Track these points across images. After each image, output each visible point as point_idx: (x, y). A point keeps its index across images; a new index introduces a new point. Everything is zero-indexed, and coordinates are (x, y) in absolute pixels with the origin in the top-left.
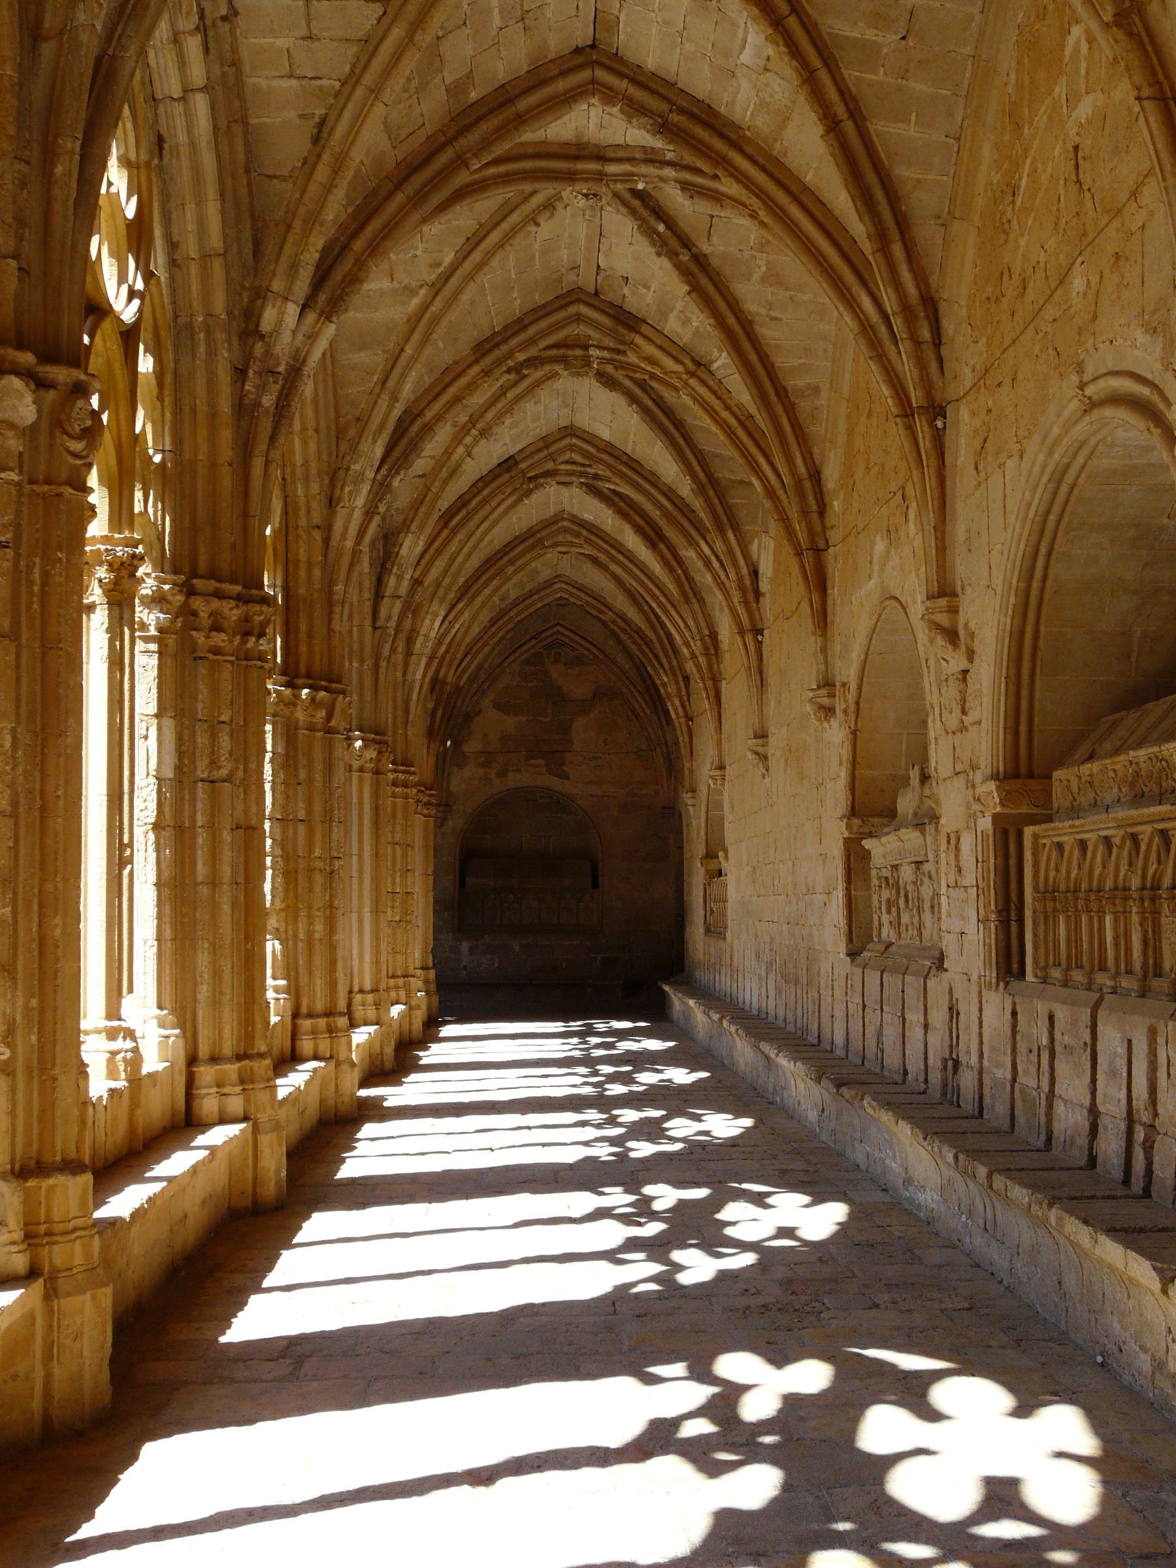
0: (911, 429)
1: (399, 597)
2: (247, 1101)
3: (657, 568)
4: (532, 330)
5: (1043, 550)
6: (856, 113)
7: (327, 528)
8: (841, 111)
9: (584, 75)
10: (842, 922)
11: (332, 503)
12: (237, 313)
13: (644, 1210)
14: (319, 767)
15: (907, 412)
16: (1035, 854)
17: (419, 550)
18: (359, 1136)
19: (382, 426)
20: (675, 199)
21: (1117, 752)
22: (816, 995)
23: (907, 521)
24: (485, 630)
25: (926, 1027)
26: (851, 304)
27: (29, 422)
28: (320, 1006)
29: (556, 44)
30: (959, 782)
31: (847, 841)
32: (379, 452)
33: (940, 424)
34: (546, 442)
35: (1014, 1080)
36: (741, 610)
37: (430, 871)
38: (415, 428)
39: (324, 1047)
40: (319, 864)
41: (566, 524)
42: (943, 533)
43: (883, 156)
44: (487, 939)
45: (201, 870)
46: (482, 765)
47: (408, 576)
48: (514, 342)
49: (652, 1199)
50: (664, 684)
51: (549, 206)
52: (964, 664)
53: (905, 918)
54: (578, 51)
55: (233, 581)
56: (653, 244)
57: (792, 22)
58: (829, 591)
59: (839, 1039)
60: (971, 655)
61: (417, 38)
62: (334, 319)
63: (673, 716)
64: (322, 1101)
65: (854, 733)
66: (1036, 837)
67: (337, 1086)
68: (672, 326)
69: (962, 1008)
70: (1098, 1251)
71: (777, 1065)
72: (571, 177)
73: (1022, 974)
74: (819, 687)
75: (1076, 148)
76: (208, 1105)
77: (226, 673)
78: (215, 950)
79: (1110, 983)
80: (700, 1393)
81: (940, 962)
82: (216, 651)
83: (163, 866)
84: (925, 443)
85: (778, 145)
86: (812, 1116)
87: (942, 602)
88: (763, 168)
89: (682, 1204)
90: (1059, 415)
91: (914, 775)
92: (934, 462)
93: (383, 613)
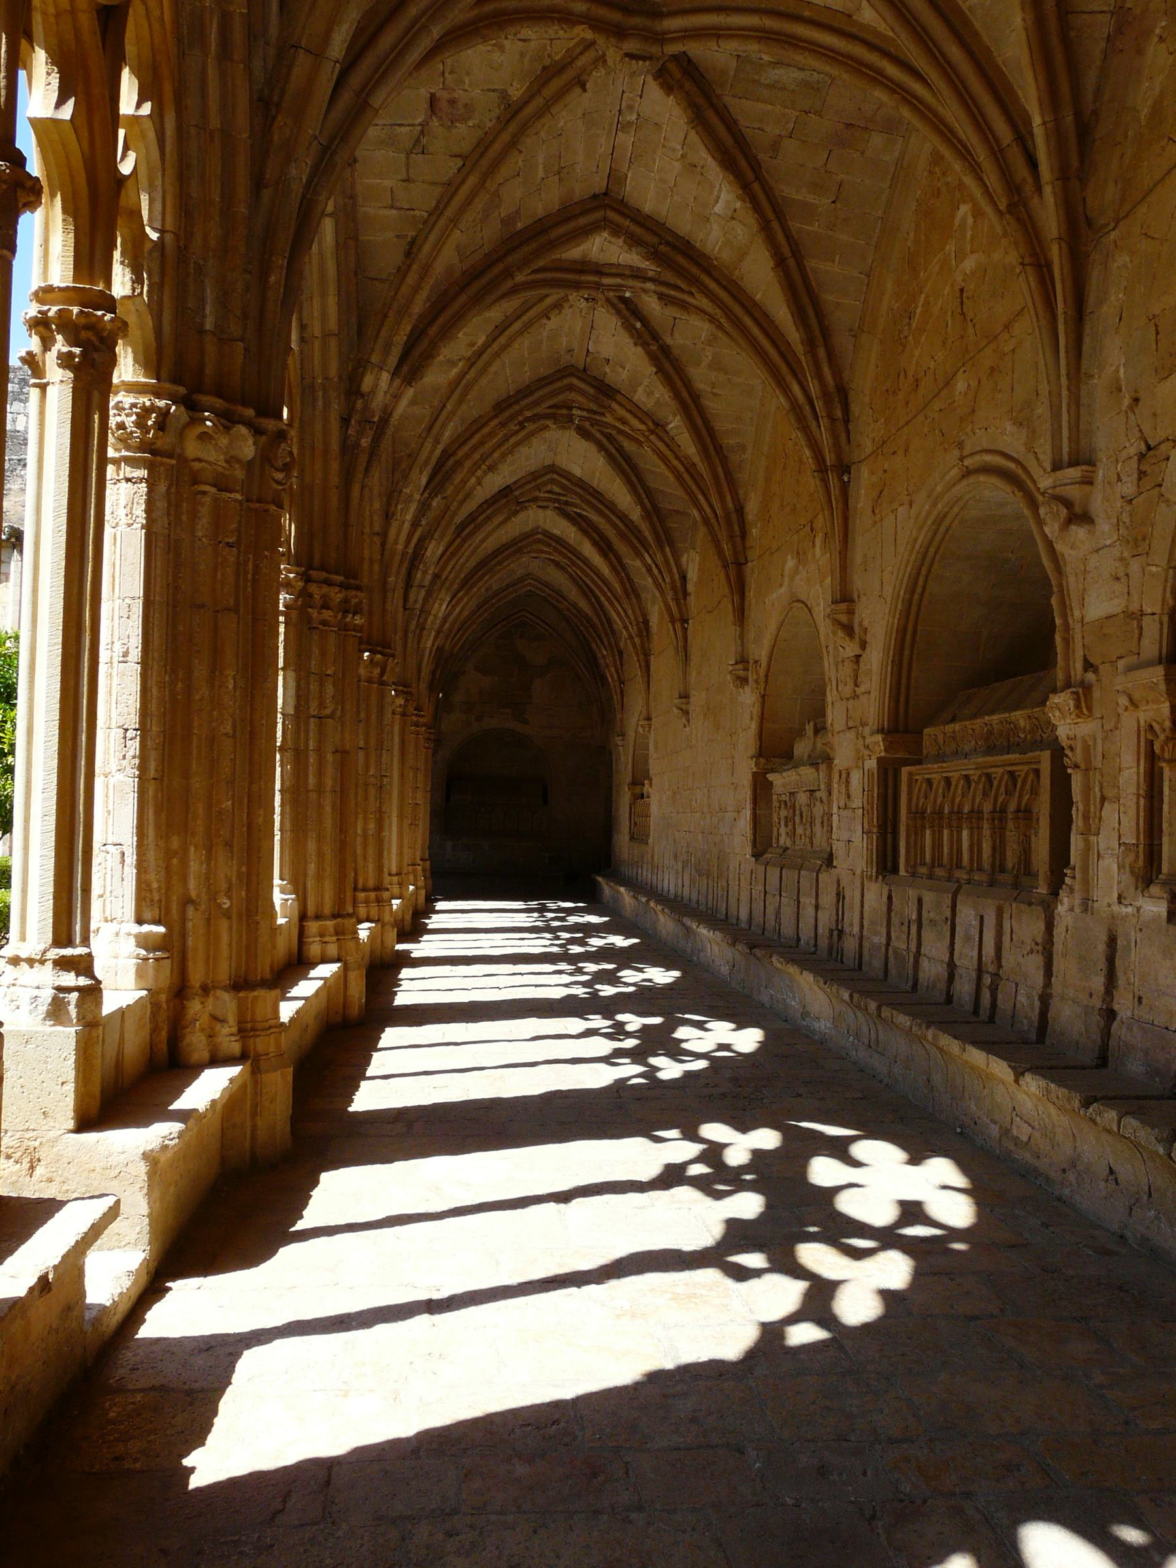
0: (825, 481)
1: (424, 587)
2: (340, 948)
3: (606, 571)
4: (538, 394)
5: (924, 572)
6: (797, 254)
7: (384, 535)
9: (600, 214)
10: (749, 834)
11: (388, 516)
12: (344, 377)
13: (619, 1031)
14: (374, 710)
15: (822, 468)
16: (910, 786)
17: (440, 552)
18: (400, 976)
19: (426, 462)
20: (651, 304)
21: (974, 716)
22: (725, 884)
23: (814, 546)
24: (473, 612)
25: (817, 907)
26: (786, 391)
27: (249, 458)
28: (371, 883)
29: (580, 191)
30: (851, 735)
31: (754, 774)
32: (424, 481)
33: (846, 479)
34: (534, 476)
35: (888, 944)
36: (672, 604)
37: (429, 788)
38: (450, 463)
39: (374, 912)
40: (372, 780)
41: (540, 536)
42: (846, 555)
43: (813, 284)
45: (312, 780)
47: (431, 572)
48: (524, 403)
49: (624, 1023)
50: (604, 657)
51: (558, 306)
52: (858, 651)
53: (799, 831)
54: (595, 196)
55: (337, 573)
56: (632, 336)
57: (756, 186)
58: (747, 594)
59: (744, 915)
60: (863, 645)
61: (488, 184)
62: (413, 384)
63: (610, 680)
64: (372, 952)
65: (763, 696)
66: (910, 774)
67: (382, 941)
68: (640, 396)
69: (847, 893)
70: (965, 1056)
71: (695, 933)
72: (577, 286)
73: (895, 870)
74: (737, 663)
75: (962, 290)
76: (314, 949)
77: (332, 640)
78: (320, 839)
79: (965, 876)
80: (693, 1149)
81: (829, 861)
82: (325, 623)
83: (285, 777)
84: (835, 492)
85: (737, 273)
86: (725, 970)
87: (844, 606)
88: (725, 288)
89: (645, 1028)
90: (942, 478)
91: (809, 728)
92: (840, 505)
93: (412, 597)
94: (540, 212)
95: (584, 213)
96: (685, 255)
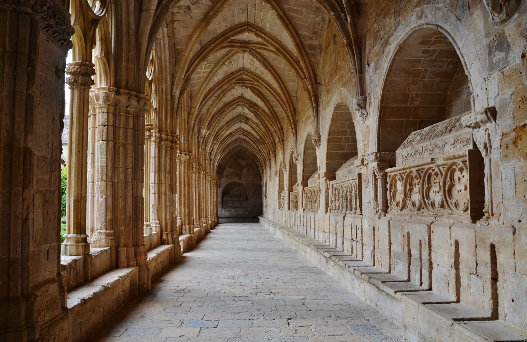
3: (255, 147)
7: (205, 149)
8: (270, 107)
11: (206, 146)
32: (212, 139)
34: (237, 130)
44: (227, 209)
46: (227, 178)
51: (236, 108)
57: (264, 99)
93: (211, 157)
94: (230, 100)
95: (237, 99)
96: (255, 106)
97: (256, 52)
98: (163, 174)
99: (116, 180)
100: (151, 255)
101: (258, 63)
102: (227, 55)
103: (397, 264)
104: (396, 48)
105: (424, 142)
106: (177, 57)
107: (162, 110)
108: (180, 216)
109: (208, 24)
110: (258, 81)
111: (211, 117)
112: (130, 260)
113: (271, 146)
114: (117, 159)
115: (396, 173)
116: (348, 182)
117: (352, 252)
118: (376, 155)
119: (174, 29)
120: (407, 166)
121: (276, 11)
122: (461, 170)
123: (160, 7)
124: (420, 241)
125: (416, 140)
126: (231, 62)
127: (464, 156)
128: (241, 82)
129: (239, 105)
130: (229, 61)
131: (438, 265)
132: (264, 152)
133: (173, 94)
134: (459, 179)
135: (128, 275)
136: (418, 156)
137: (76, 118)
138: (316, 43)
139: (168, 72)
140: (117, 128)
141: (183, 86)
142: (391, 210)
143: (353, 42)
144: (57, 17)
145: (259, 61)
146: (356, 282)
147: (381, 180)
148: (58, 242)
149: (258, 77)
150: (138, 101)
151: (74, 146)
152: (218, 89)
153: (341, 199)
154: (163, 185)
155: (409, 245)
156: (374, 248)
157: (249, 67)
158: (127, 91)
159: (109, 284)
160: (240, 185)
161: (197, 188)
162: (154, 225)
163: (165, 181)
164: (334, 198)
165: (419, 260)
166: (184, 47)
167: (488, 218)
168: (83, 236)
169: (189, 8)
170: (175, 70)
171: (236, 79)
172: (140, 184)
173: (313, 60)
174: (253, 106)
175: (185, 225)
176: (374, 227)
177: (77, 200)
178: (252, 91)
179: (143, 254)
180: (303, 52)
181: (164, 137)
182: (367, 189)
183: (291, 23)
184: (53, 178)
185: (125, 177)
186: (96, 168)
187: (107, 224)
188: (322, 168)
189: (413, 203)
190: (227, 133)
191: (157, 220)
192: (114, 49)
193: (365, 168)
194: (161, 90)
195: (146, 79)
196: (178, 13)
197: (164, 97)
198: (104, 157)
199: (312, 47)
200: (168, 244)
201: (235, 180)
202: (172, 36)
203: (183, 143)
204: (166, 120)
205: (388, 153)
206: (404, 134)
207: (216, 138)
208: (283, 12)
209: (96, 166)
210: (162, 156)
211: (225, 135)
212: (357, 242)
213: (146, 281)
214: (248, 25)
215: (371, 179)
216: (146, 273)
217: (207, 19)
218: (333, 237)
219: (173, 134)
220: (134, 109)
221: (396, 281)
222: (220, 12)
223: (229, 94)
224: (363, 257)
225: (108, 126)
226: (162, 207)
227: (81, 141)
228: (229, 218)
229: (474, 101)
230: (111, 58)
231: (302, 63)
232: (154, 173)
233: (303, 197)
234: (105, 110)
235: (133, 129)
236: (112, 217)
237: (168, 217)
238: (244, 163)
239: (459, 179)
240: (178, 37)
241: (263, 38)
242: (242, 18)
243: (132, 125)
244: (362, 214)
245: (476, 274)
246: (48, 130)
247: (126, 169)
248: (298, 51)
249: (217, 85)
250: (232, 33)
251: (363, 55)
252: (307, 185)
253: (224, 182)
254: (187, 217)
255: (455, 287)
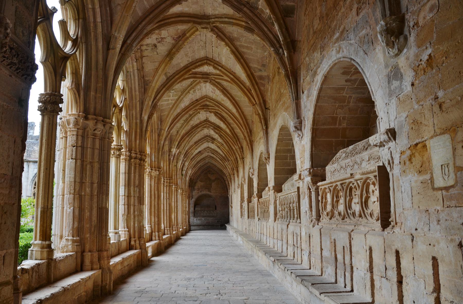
3: (222, 163)
7: (176, 166)
11: (177, 162)
24: (198, 170)
32: (183, 156)
34: (205, 149)
44: (199, 218)
51: (203, 129)
57: (226, 122)
84: (242, 162)
93: (183, 172)
94: (197, 123)
97: (216, 82)
98: (132, 187)
99: (83, 194)
100: (117, 259)
101: (218, 91)
102: (192, 85)
103: (327, 268)
104: (322, 78)
105: (347, 159)
106: (146, 87)
107: (132, 132)
108: (150, 225)
109: (171, 59)
110: (219, 107)
111: (180, 138)
112: (94, 264)
113: (234, 163)
114: (84, 175)
115: (325, 186)
116: (291, 194)
117: (294, 257)
118: (310, 171)
119: (143, 63)
120: (333, 180)
121: (229, 47)
122: (374, 184)
123: (125, 46)
124: (344, 247)
125: (342, 157)
126: (195, 90)
127: (374, 171)
128: (205, 107)
129: (205, 127)
130: (193, 90)
131: (357, 268)
132: (229, 168)
133: (142, 119)
134: (373, 192)
135: (90, 277)
136: (342, 171)
137: (45, 140)
138: (264, 74)
139: (138, 99)
140: (85, 149)
141: (150, 112)
142: (322, 219)
143: (290, 73)
144: (20, 56)
145: (219, 90)
146: (295, 284)
147: (314, 192)
148: (15, 248)
149: (219, 104)
150: (104, 125)
151: (43, 164)
152: (185, 114)
153: (286, 209)
154: (132, 197)
155: (335, 251)
156: (310, 253)
157: (211, 95)
158: (95, 117)
159: (68, 285)
160: (210, 196)
161: (168, 200)
162: (123, 233)
163: (134, 194)
164: (281, 208)
165: (343, 265)
166: (151, 79)
167: (393, 226)
168: (47, 243)
169: (155, 46)
170: (144, 98)
171: (200, 105)
172: (104, 197)
173: (262, 88)
174: (216, 128)
175: (155, 232)
176: (309, 234)
177: (44, 211)
178: (216, 115)
179: (106, 259)
180: (254, 81)
181: (133, 155)
182: (304, 201)
183: (242, 57)
184: (13, 193)
185: (92, 191)
186: (66, 183)
187: (74, 232)
188: (271, 183)
189: (339, 213)
190: (197, 151)
191: (126, 228)
192: (84, 81)
193: (302, 182)
194: (131, 115)
195: (116, 106)
196: (147, 50)
197: (134, 121)
198: (73, 173)
199: (261, 78)
200: (136, 249)
201: (204, 192)
202: (141, 69)
203: (153, 160)
204: (136, 141)
205: (320, 168)
206: (334, 152)
207: (186, 156)
208: (235, 48)
209: (66, 181)
210: (131, 172)
211: (195, 154)
212: (298, 247)
213: (108, 282)
214: (207, 60)
215: (307, 192)
216: (108, 275)
217: (170, 55)
218: (280, 243)
219: (142, 153)
220: (100, 132)
221: (324, 283)
222: (181, 48)
223: (196, 118)
224: (302, 261)
225: (77, 146)
226: (130, 217)
227: (49, 160)
228: (200, 225)
229: (379, 123)
230: (80, 89)
231: (253, 91)
232: (124, 187)
233: (258, 208)
234: (75, 133)
235: (99, 149)
236: (79, 225)
237: (136, 225)
238: (212, 177)
239: (373, 192)
240: (147, 70)
241: (220, 70)
242: (202, 54)
243: (98, 146)
244: (300, 223)
245: (386, 277)
246: (9, 151)
247: (92, 183)
248: (249, 81)
249: (184, 110)
250: (193, 66)
251: (298, 84)
252: (261, 197)
253: (196, 194)
254: (156, 226)
255: (370, 289)
